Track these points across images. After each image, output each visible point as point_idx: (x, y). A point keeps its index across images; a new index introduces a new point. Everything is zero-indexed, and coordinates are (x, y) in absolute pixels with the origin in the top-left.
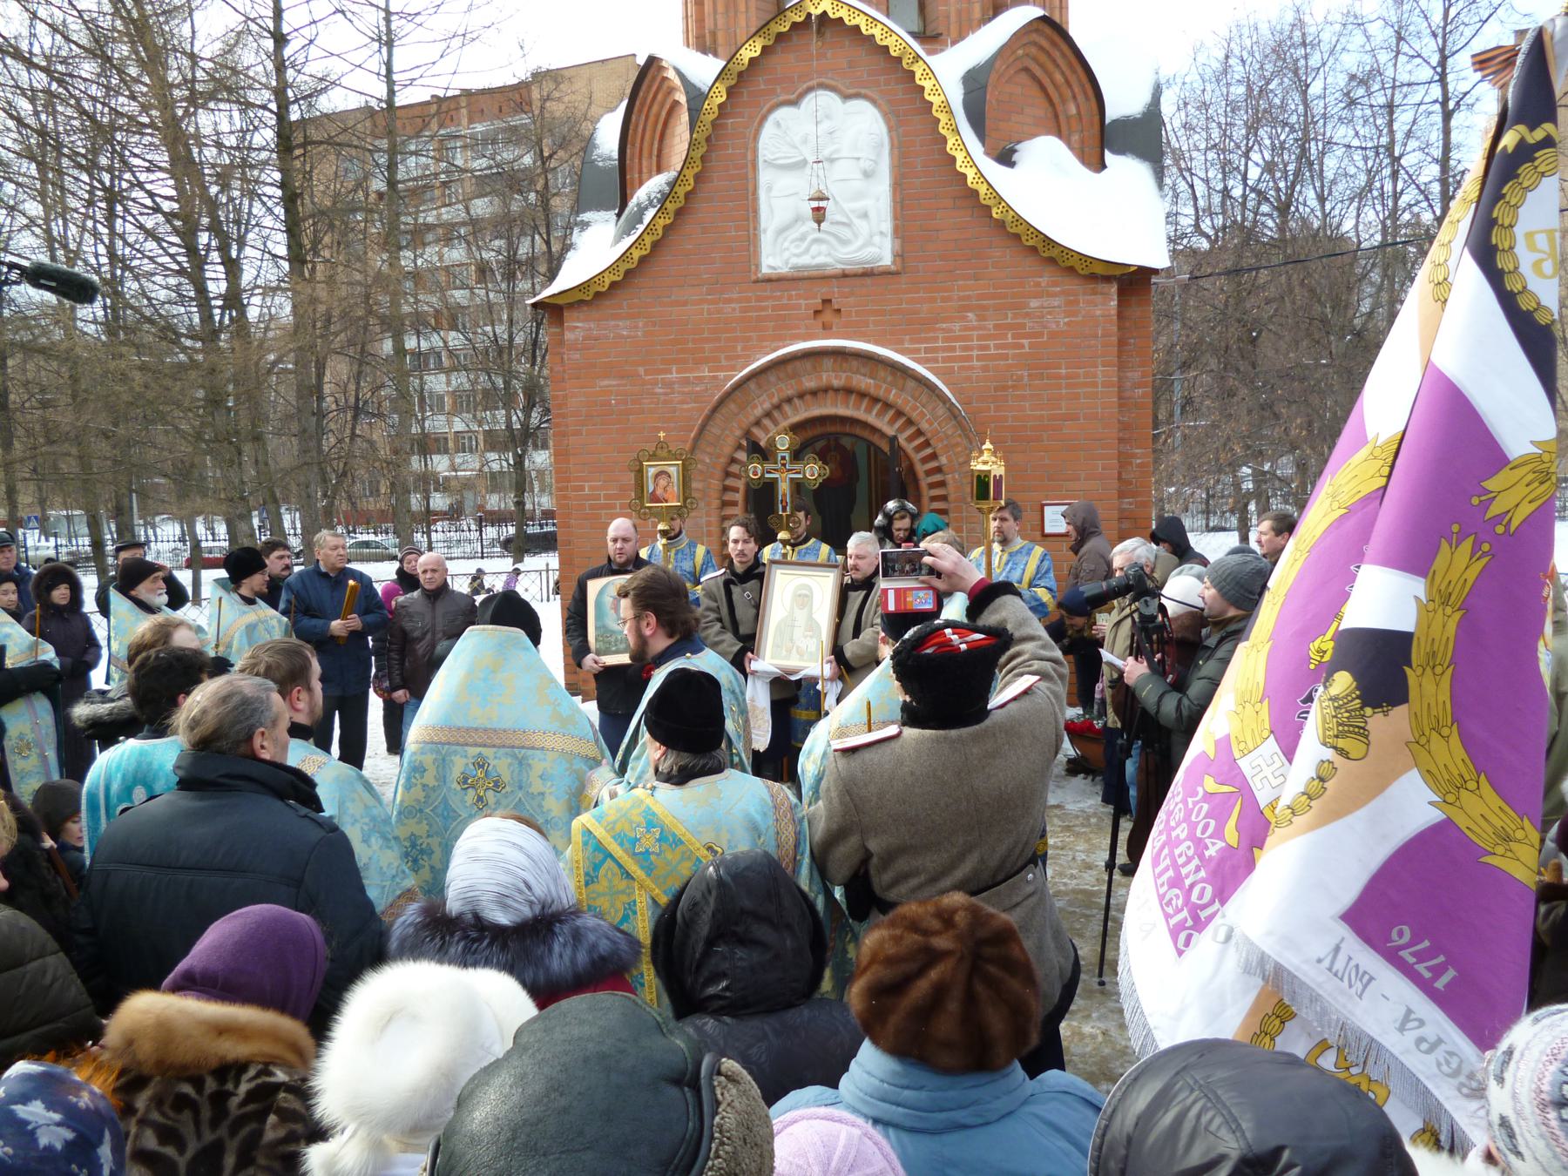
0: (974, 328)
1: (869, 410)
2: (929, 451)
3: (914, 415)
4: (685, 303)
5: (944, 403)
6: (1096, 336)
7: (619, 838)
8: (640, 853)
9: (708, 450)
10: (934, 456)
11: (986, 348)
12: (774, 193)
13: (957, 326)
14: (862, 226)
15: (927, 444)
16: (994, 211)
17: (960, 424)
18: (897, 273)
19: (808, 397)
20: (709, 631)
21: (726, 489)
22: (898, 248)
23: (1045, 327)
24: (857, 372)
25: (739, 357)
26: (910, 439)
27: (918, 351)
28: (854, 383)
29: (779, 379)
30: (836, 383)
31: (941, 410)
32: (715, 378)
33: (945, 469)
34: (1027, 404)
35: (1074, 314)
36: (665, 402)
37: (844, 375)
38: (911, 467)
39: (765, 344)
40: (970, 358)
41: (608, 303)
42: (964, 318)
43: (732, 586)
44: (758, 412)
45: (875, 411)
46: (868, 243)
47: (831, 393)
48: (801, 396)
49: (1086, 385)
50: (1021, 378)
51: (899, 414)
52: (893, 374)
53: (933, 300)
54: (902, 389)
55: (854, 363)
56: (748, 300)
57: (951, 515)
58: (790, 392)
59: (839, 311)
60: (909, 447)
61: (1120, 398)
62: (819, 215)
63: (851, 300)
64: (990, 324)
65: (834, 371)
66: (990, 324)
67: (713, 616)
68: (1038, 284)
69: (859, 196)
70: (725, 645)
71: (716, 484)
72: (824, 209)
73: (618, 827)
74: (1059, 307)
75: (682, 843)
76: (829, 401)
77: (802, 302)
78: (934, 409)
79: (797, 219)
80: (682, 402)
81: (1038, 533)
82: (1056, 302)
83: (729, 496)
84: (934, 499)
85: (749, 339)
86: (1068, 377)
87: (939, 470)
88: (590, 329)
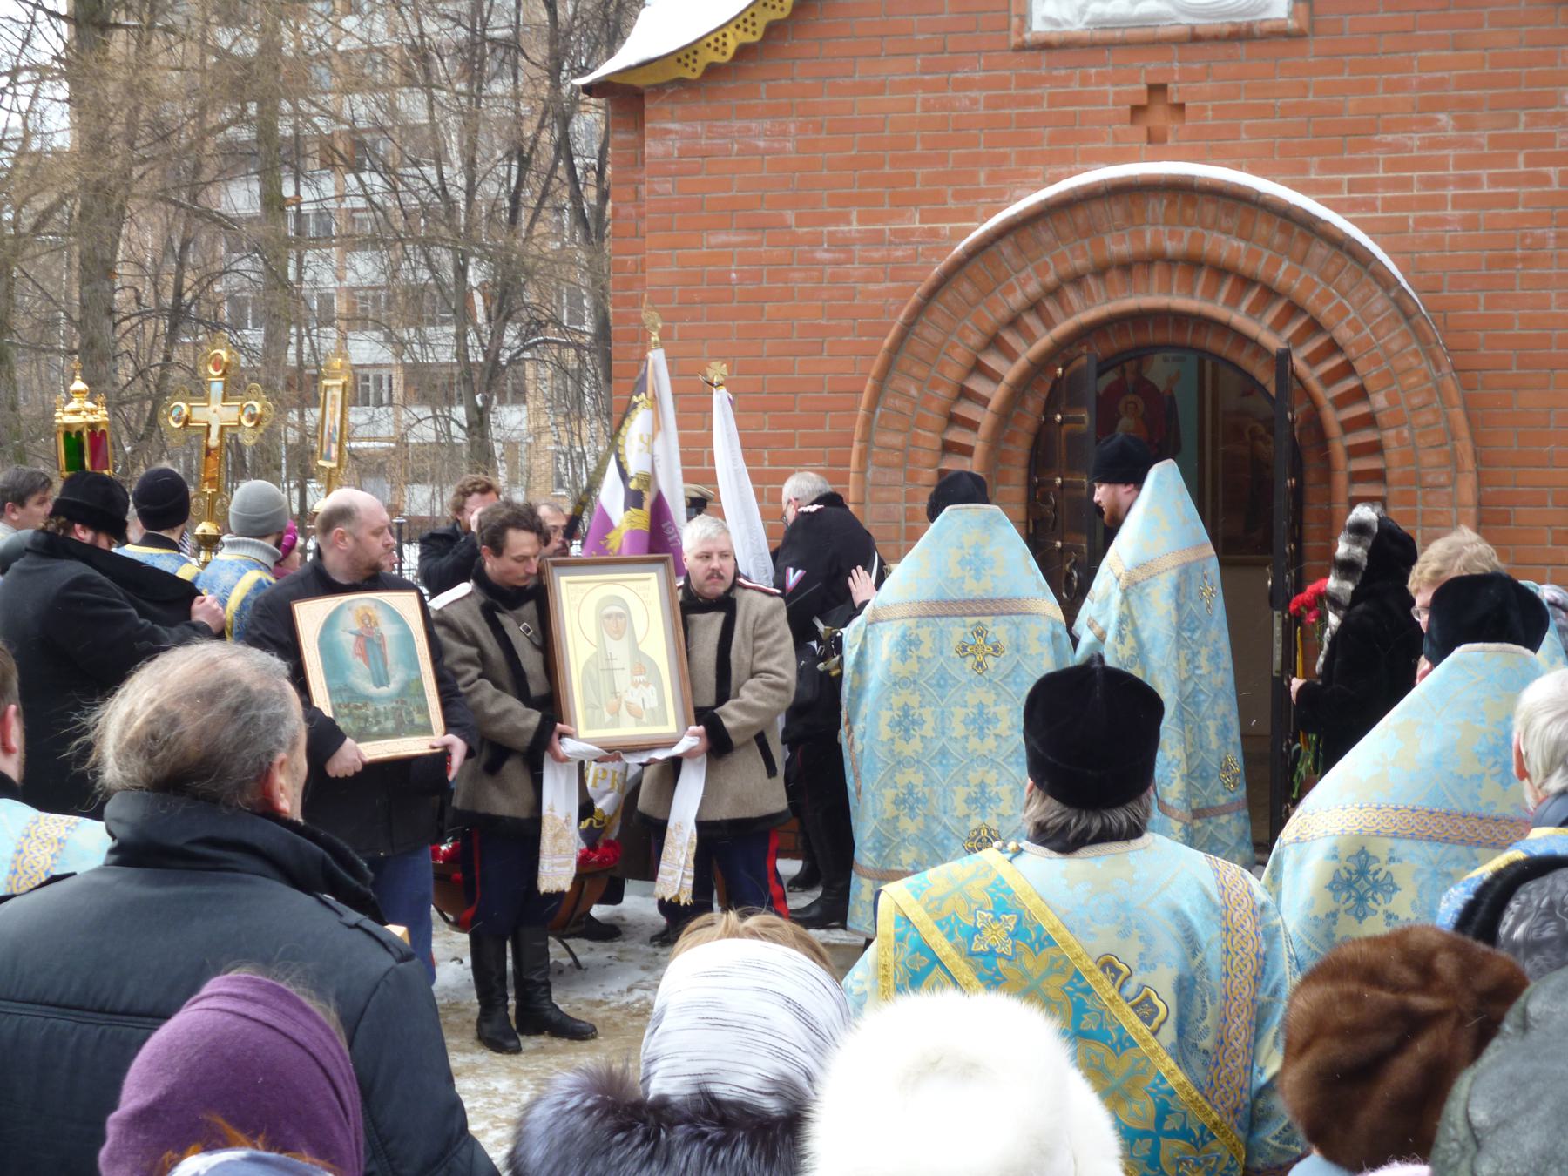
0: (1448, 144)
1: (1233, 302)
2: (1350, 383)
3: (1325, 312)
4: (880, 89)
5: (1387, 289)
7: (948, 926)
8: (981, 953)
9: (916, 370)
10: (1361, 394)
11: (1474, 181)
13: (1415, 139)
15: (1347, 369)
19: (1114, 275)
24: (1215, 226)
25: (979, 193)
26: (1313, 360)
27: (1335, 186)
28: (1207, 247)
29: (1059, 237)
30: (1170, 247)
31: (1379, 303)
32: (934, 233)
33: (1382, 419)
34: (1553, 294)
36: (835, 278)
37: (1187, 232)
39: (1033, 169)
40: (1438, 203)
41: (731, 85)
44: (1016, 299)
45: (1244, 306)
47: (1158, 269)
48: (1101, 271)
50: (1541, 243)
51: (1294, 309)
52: (1283, 229)
53: (1368, 88)
54: (1303, 261)
55: (1209, 209)
56: (1004, 83)
58: (1079, 263)
59: (1180, 107)
63: (1208, 85)
64: (1482, 136)
65: (1166, 223)
66: (1482, 136)
71: (930, 439)
73: (947, 908)
75: (1052, 943)
76: (1155, 281)
77: (1110, 89)
78: (1365, 300)
80: (868, 279)
85: (1004, 158)
87: (1369, 421)
88: (695, 136)
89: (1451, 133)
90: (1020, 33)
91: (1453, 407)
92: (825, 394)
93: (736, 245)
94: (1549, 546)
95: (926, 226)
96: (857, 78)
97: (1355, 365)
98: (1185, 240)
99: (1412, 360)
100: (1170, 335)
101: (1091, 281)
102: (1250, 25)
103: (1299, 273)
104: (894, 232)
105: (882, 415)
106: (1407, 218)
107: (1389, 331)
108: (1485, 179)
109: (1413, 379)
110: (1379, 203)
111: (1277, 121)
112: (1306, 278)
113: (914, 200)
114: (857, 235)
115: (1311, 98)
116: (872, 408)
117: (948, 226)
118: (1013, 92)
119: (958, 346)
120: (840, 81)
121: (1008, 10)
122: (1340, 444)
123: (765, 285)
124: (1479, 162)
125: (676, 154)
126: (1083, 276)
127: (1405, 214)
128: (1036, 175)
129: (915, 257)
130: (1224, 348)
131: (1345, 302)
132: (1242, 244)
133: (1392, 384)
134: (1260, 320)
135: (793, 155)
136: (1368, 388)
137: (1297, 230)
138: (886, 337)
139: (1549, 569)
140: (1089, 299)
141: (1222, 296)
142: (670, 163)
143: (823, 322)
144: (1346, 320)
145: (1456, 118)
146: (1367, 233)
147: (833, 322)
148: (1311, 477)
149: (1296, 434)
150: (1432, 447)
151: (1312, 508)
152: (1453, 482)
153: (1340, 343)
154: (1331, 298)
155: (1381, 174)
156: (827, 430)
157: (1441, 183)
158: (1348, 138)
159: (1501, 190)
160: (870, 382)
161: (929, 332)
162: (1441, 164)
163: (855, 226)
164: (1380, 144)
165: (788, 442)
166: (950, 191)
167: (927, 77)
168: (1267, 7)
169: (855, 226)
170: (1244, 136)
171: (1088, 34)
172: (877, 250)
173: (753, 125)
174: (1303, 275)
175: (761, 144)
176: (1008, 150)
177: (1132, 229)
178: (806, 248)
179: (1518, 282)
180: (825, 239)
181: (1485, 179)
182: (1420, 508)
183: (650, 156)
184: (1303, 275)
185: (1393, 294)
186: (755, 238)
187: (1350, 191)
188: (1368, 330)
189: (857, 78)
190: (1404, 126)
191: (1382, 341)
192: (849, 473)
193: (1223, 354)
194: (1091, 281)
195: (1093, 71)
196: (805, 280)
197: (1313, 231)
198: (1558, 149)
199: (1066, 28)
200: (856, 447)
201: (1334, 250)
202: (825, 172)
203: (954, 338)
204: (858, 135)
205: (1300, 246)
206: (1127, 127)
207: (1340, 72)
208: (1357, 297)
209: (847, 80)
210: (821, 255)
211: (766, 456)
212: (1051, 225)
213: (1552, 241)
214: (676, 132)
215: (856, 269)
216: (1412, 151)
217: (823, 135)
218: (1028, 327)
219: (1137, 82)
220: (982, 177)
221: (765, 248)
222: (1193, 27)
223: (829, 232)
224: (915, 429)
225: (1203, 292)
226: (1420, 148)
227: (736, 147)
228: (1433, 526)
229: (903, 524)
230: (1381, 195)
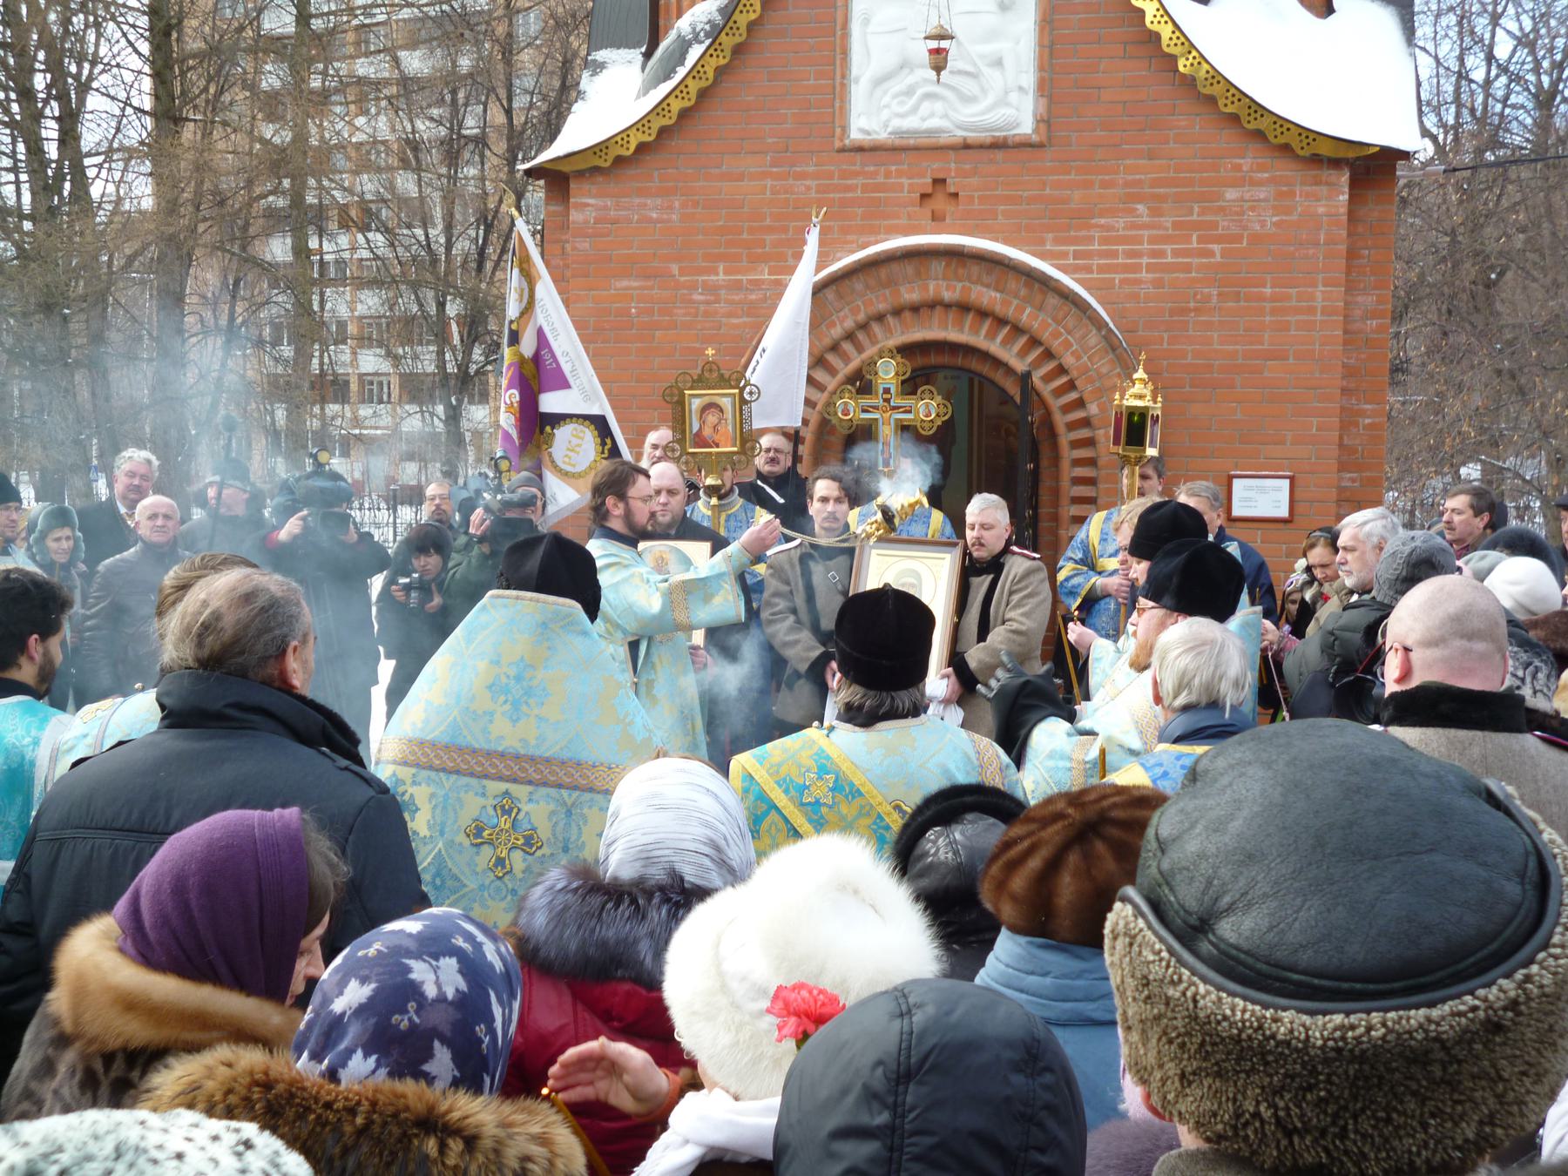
1: (991, 336)
2: (1073, 396)
3: (1055, 345)
4: (740, 177)
5: (1099, 329)
6: (1317, 244)
7: (785, 784)
8: (810, 803)
11: (1162, 254)
12: (871, 28)
13: (1120, 222)
14: (993, 77)
15: (1071, 385)
16: (1181, 63)
17: (1119, 358)
18: (1040, 146)
19: (907, 315)
20: (778, 626)
22: (1042, 110)
23: (1245, 228)
24: (978, 281)
26: (1047, 378)
27: (1064, 255)
28: (973, 297)
29: (867, 287)
30: (947, 296)
31: (1093, 338)
33: (1095, 422)
34: (1216, 335)
35: (1288, 211)
36: (706, 314)
37: (959, 286)
39: (850, 238)
40: (1136, 268)
42: (1132, 212)
43: (812, 564)
44: (837, 332)
45: (999, 339)
46: (1002, 102)
47: (938, 308)
48: (897, 312)
49: (1298, 311)
50: (1207, 299)
51: (1034, 342)
52: (1026, 285)
53: (1088, 185)
54: (1040, 308)
55: (975, 269)
56: (830, 176)
57: (1102, 486)
59: (956, 195)
60: (1046, 390)
61: (1346, 332)
62: (939, 60)
63: (974, 181)
64: (1167, 221)
65: (944, 279)
66: (1167, 221)
67: (782, 604)
68: (1238, 168)
69: (992, 35)
70: (799, 647)
72: (945, 51)
73: (784, 771)
74: (1265, 200)
77: (905, 181)
79: (905, 65)
80: (730, 315)
82: (1262, 193)
84: (1077, 462)
86: (1274, 299)
87: (1086, 423)
88: (605, 208)
90: (842, 140)
97: (1077, 383)
100: (946, 359)
101: (890, 319)
102: (1005, 138)
104: (750, 281)
107: (1100, 359)
110: (1095, 268)
111: (1024, 207)
113: (764, 258)
115: (1048, 191)
121: (833, 122)
122: (1065, 438)
124: (1166, 239)
128: (852, 242)
130: (985, 369)
132: (998, 295)
137: (1037, 285)
140: (889, 331)
141: (983, 332)
146: (1087, 289)
148: (1044, 463)
151: (1046, 483)
154: (1061, 334)
155: (1096, 247)
159: (1180, 260)
163: (721, 276)
168: (1018, 125)
169: (721, 276)
171: (890, 142)
173: (649, 201)
175: (655, 215)
183: (574, 222)
186: (649, 283)
188: (1085, 358)
190: (1111, 212)
194: (890, 319)
195: (893, 168)
196: (685, 315)
199: (875, 136)
201: (1062, 301)
202: (700, 237)
205: (1039, 297)
206: (917, 209)
207: (1069, 173)
208: (1077, 336)
209: (717, 170)
210: (697, 297)
215: (722, 307)
219: (924, 176)
222: (965, 139)
225: (971, 327)
230: (1096, 262)
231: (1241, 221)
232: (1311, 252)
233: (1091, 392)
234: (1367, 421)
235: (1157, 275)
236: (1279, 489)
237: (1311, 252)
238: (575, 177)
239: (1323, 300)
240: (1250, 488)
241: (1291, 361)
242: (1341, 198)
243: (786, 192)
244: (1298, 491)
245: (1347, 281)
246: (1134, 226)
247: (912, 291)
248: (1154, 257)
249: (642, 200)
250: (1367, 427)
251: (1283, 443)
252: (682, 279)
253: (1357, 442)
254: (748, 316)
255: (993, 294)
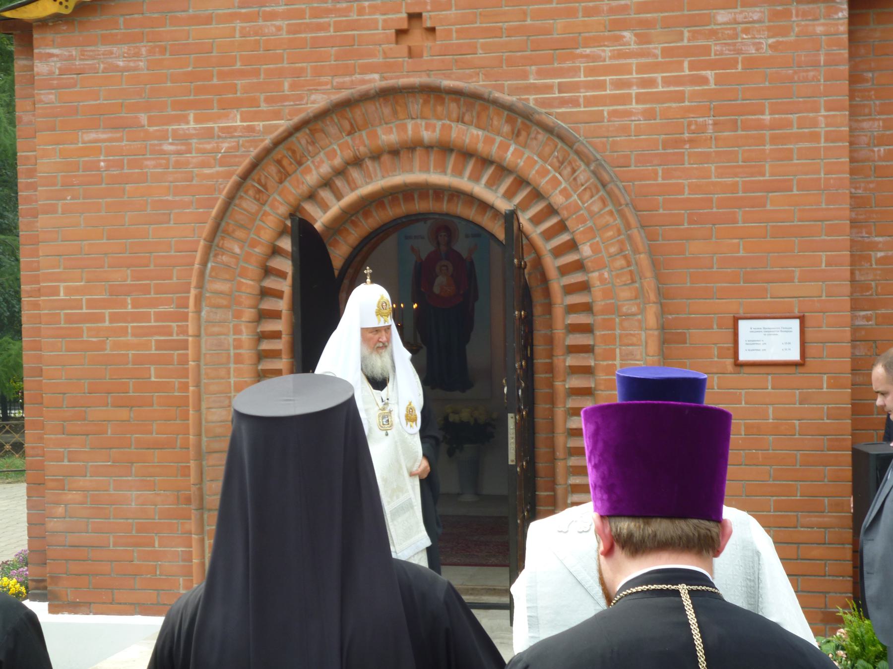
2: (564, 237)
3: (543, 183)
4: (208, 20)
5: (588, 164)
6: (816, 65)
9: (240, 234)
11: (652, 83)
15: (562, 227)
17: (610, 194)
19: (386, 158)
21: (265, 293)
23: (739, 52)
24: (460, 120)
26: (536, 220)
28: (454, 135)
30: (427, 136)
31: (583, 174)
32: (251, 129)
33: (589, 264)
35: (785, 31)
36: (178, 164)
37: (439, 124)
38: (538, 262)
39: (323, 79)
40: (625, 99)
41: (97, 19)
42: (618, 39)
44: (312, 179)
45: (484, 180)
47: (419, 152)
48: (376, 156)
49: (800, 138)
50: (702, 128)
51: (521, 182)
53: (571, 13)
56: (300, 14)
59: (432, 30)
60: (535, 232)
61: (852, 160)
64: (656, 48)
65: (423, 118)
66: (656, 48)
71: (249, 285)
74: (759, 21)
76: (417, 163)
77: (380, 17)
80: (203, 165)
81: (730, 361)
83: (269, 304)
84: (572, 309)
87: (579, 266)
88: (71, 58)
89: (634, 47)
91: (640, 253)
92: (173, 253)
93: (104, 141)
94: (716, 359)
95: (245, 124)
96: (191, 12)
97: (567, 223)
98: (438, 130)
99: (609, 219)
101: (369, 163)
103: (523, 154)
104: (222, 129)
105: (212, 267)
106: (603, 111)
107: (592, 196)
108: (659, 80)
109: (610, 233)
112: (529, 157)
113: (236, 104)
114: (194, 132)
115: (529, 22)
116: (204, 263)
117: (261, 124)
118: (307, 21)
119: (270, 215)
120: (178, 14)
122: (557, 284)
123: (126, 171)
125: (57, 72)
126: (363, 160)
127: (601, 108)
128: (326, 84)
129: (237, 148)
130: (471, 214)
131: (557, 175)
132: (480, 133)
133: (595, 237)
134: (496, 191)
135: (146, 72)
136: (577, 241)
137: (520, 120)
138: (213, 208)
139: (716, 376)
140: (369, 178)
142: (54, 79)
143: (170, 198)
144: (559, 189)
145: (636, 35)
147: (177, 198)
148: (538, 310)
149: (527, 277)
150: (625, 285)
151: (540, 333)
152: (642, 311)
153: (556, 207)
154: (548, 172)
155: (583, 79)
156: (175, 280)
157: (627, 84)
158: (557, 51)
159: (672, 89)
160: (202, 243)
161: (248, 204)
162: (626, 70)
164: (582, 56)
165: (146, 290)
166: (262, 97)
167: (243, 11)
169: (192, 125)
170: (480, 51)
172: (209, 143)
173: (115, 49)
174: (526, 156)
175: (121, 64)
176: (304, 65)
177: (398, 122)
178: (156, 142)
179: (686, 158)
180: (170, 134)
181: (659, 80)
182: (618, 332)
183: (38, 74)
184: (526, 156)
185: (592, 168)
186: (118, 135)
187: (560, 92)
188: (575, 197)
189: (191, 12)
190: (597, 41)
191: (586, 205)
192: (188, 312)
193: (471, 218)
194: (369, 163)
196: (155, 167)
197: (531, 121)
198: (713, 57)
200: (193, 292)
201: (547, 135)
203: (267, 208)
204: (192, 56)
206: (393, 46)
210: (167, 147)
211: (129, 301)
212: (336, 120)
213: (711, 127)
214: (57, 56)
215: (194, 157)
216: (604, 60)
217: (167, 56)
218: (322, 199)
220: (286, 85)
221: (125, 143)
223: (173, 129)
224: (239, 278)
225: (453, 170)
226: (611, 58)
227: (102, 66)
228: (629, 345)
229: (232, 352)
230: (582, 94)
231: (734, 44)
232: (811, 74)
233: (583, 232)
234: (880, 254)
235: (648, 106)
236: (788, 330)
237: (811, 74)
238: (38, 26)
239: (827, 125)
240: (757, 330)
241: (795, 192)
242: (840, 15)
243: (256, 34)
244: (808, 330)
245: (851, 106)
246: (620, 55)
247: (390, 131)
248: (644, 87)
249: (107, 48)
250: (879, 261)
251: (792, 281)
252: (152, 129)
253: (871, 277)
254: (221, 166)
255: (475, 131)
